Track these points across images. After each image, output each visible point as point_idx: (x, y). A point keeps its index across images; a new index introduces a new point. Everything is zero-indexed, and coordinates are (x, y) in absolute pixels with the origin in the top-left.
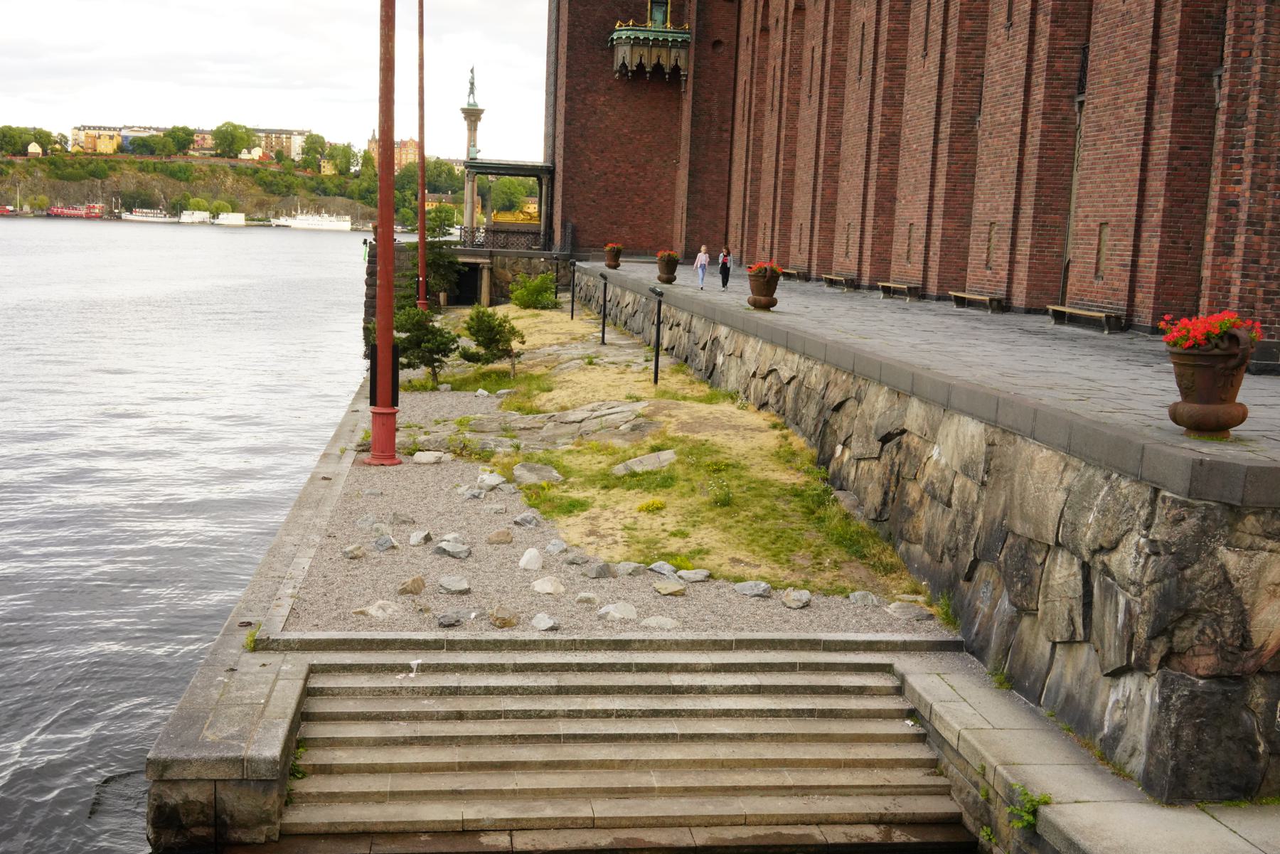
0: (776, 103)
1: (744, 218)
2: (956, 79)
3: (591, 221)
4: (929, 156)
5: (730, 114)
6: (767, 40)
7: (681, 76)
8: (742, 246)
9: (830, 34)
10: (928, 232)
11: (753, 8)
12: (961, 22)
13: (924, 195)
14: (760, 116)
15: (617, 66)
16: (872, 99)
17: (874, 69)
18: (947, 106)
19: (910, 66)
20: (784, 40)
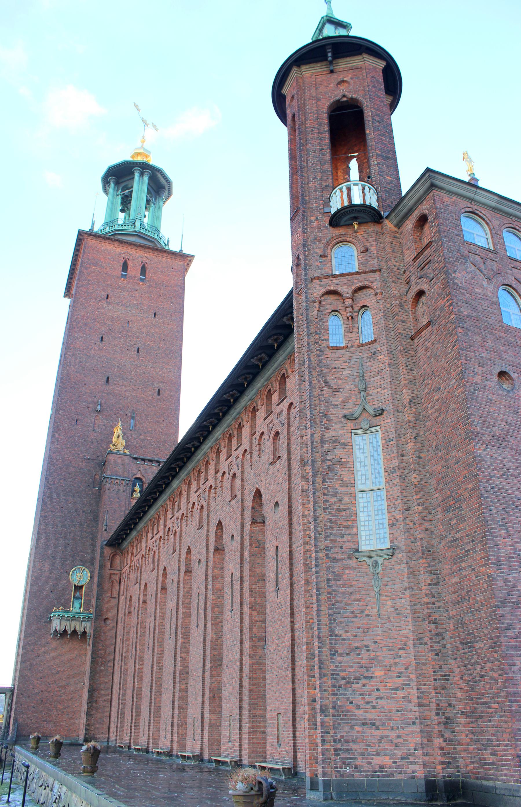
0: (134, 651)
1: (118, 716)
2: (212, 638)
3: (31, 720)
4: (201, 679)
5: (113, 657)
6: (130, 618)
7: (87, 636)
8: (117, 733)
9: (158, 615)
10: (202, 722)
11: (124, 602)
12: (213, 608)
13: (200, 701)
14: (126, 660)
15: (52, 631)
16: (176, 648)
17: (176, 633)
18: (208, 652)
19: (192, 631)
20: (138, 618)
